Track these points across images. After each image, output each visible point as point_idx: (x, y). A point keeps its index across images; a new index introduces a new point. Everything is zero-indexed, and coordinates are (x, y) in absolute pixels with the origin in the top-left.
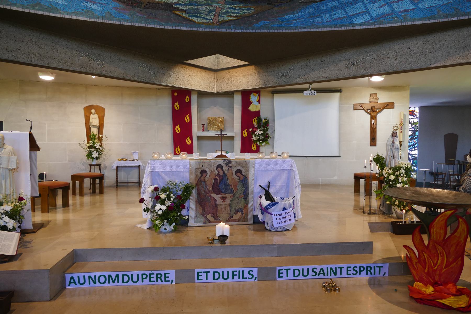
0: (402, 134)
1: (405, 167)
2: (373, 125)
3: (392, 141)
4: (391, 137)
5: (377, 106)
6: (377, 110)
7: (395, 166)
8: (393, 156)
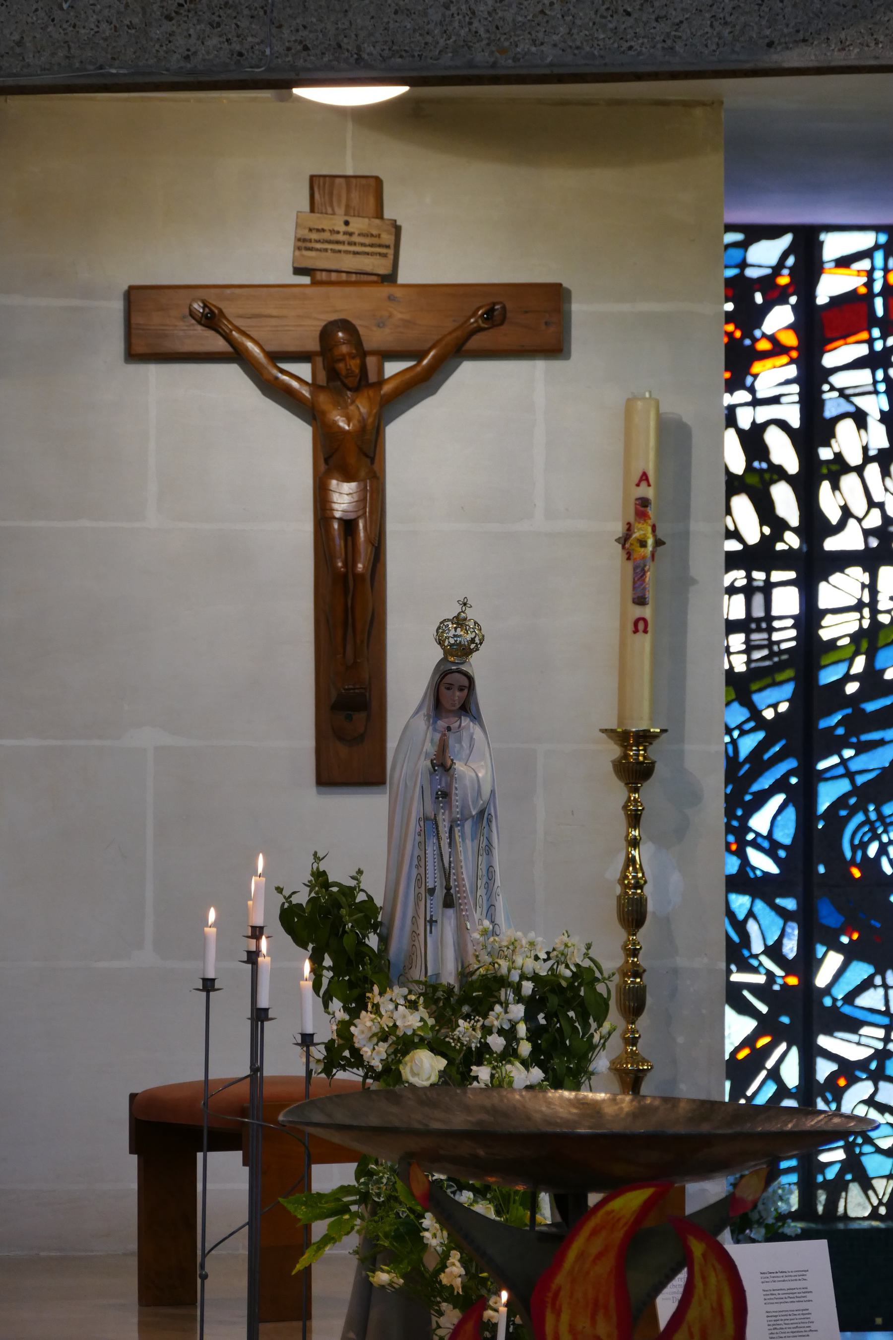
0: (645, 642)
1: (535, 978)
2: (339, 542)
3: (430, 748)
4: (428, 716)
5: (381, 325)
6: (392, 368)
7: (464, 974)
8: (448, 888)
